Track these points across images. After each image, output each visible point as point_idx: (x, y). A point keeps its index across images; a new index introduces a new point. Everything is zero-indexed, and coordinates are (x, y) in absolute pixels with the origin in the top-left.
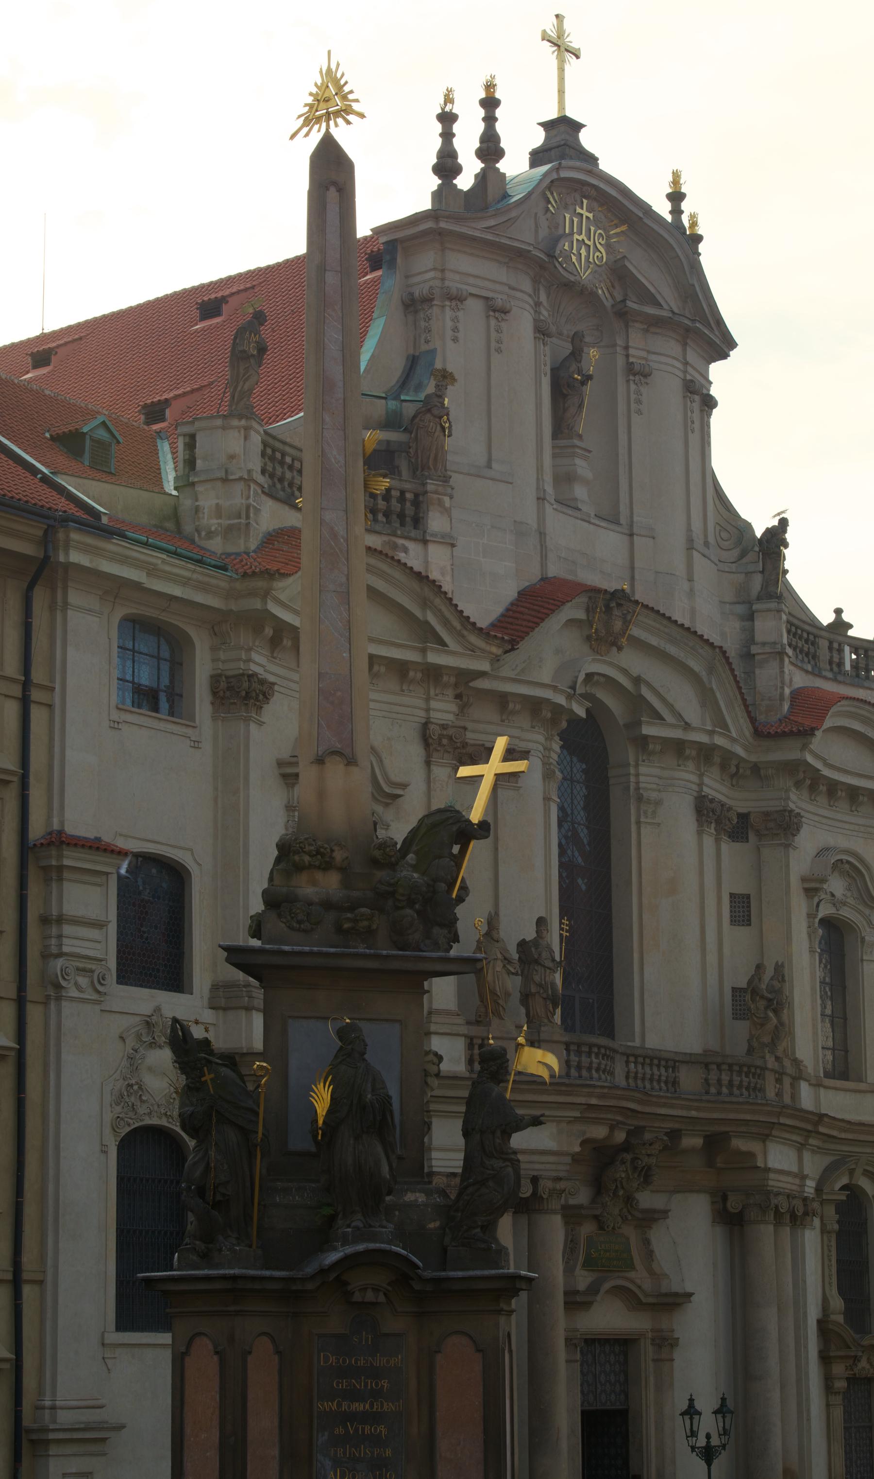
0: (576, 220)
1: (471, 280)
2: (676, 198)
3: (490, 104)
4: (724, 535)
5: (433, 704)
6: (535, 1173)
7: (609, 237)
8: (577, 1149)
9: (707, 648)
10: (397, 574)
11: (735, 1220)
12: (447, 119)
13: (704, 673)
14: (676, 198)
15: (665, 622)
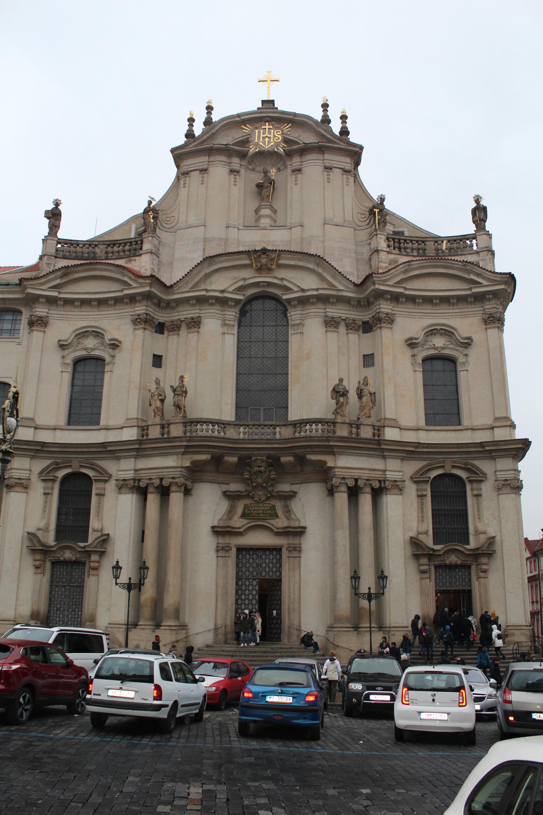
0: (262, 131)
1: (192, 166)
2: (325, 106)
3: (209, 109)
4: (363, 216)
5: (136, 309)
6: (162, 477)
7: (282, 131)
8: (188, 464)
9: (313, 257)
10: (111, 268)
11: (331, 492)
12: (191, 120)
13: (316, 268)
14: (325, 106)
15: (294, 254)
